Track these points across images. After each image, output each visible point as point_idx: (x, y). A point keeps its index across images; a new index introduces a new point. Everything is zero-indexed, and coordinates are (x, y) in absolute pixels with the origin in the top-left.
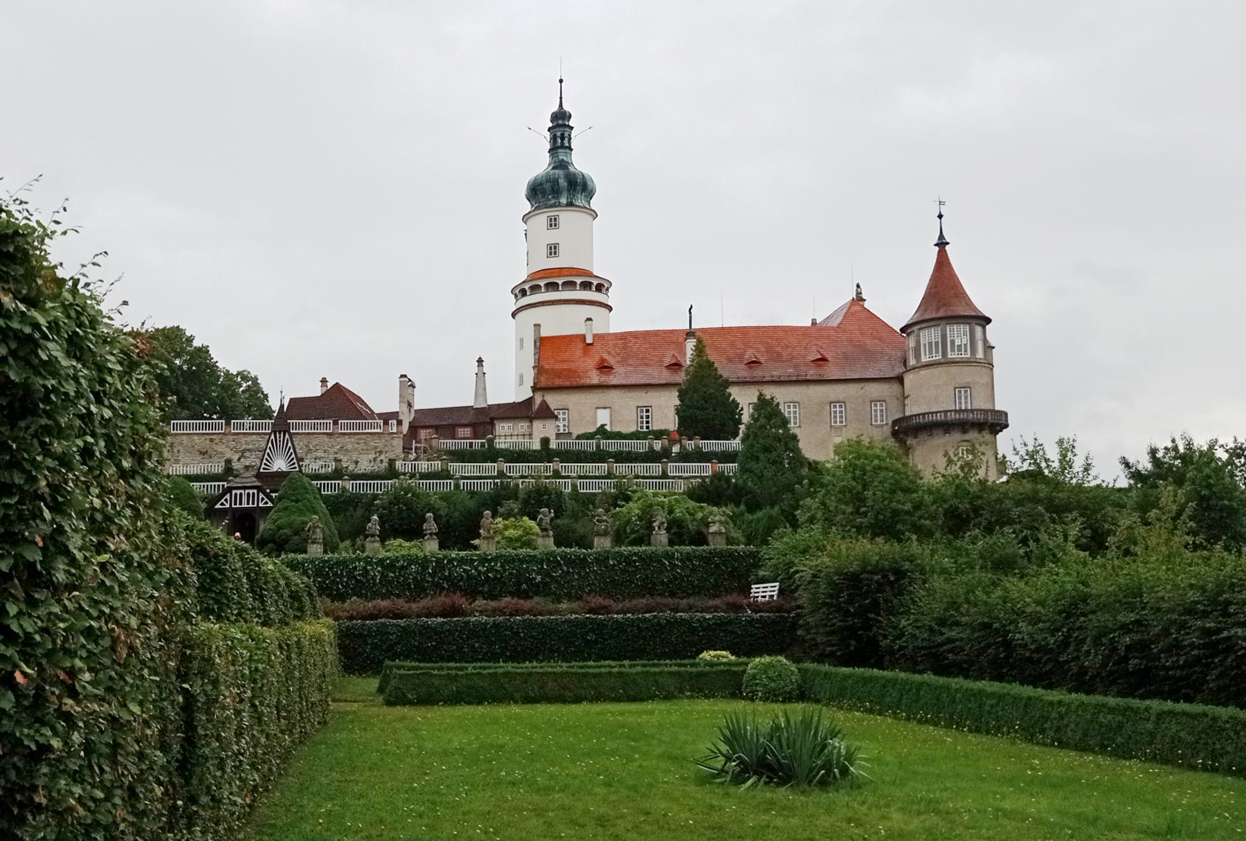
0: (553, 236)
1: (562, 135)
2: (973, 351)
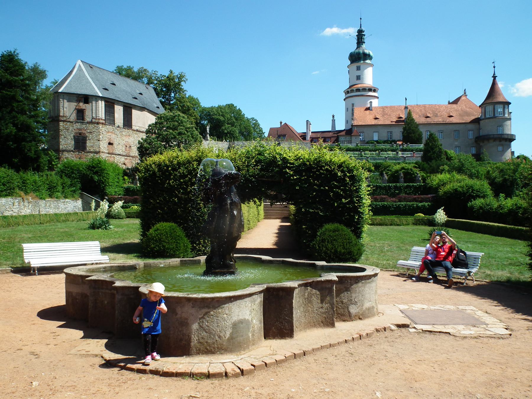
0: (358, 73)
1: (362, 38)
2: (504, 115)
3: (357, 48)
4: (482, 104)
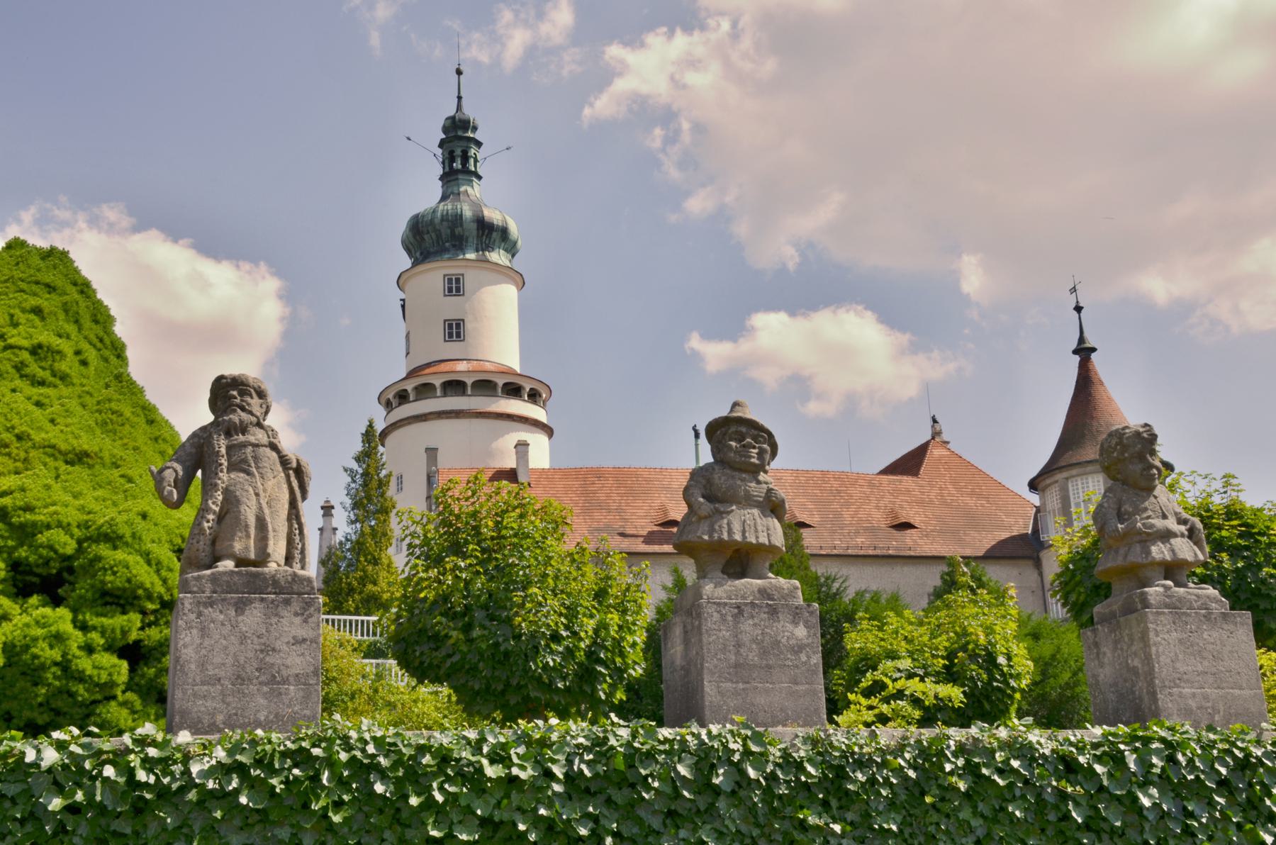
1: (465, 158)
3: (444, 198)
4: (1048, 470)
